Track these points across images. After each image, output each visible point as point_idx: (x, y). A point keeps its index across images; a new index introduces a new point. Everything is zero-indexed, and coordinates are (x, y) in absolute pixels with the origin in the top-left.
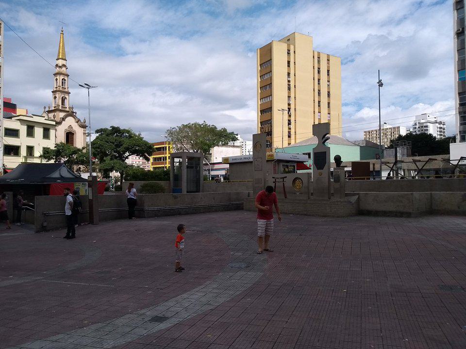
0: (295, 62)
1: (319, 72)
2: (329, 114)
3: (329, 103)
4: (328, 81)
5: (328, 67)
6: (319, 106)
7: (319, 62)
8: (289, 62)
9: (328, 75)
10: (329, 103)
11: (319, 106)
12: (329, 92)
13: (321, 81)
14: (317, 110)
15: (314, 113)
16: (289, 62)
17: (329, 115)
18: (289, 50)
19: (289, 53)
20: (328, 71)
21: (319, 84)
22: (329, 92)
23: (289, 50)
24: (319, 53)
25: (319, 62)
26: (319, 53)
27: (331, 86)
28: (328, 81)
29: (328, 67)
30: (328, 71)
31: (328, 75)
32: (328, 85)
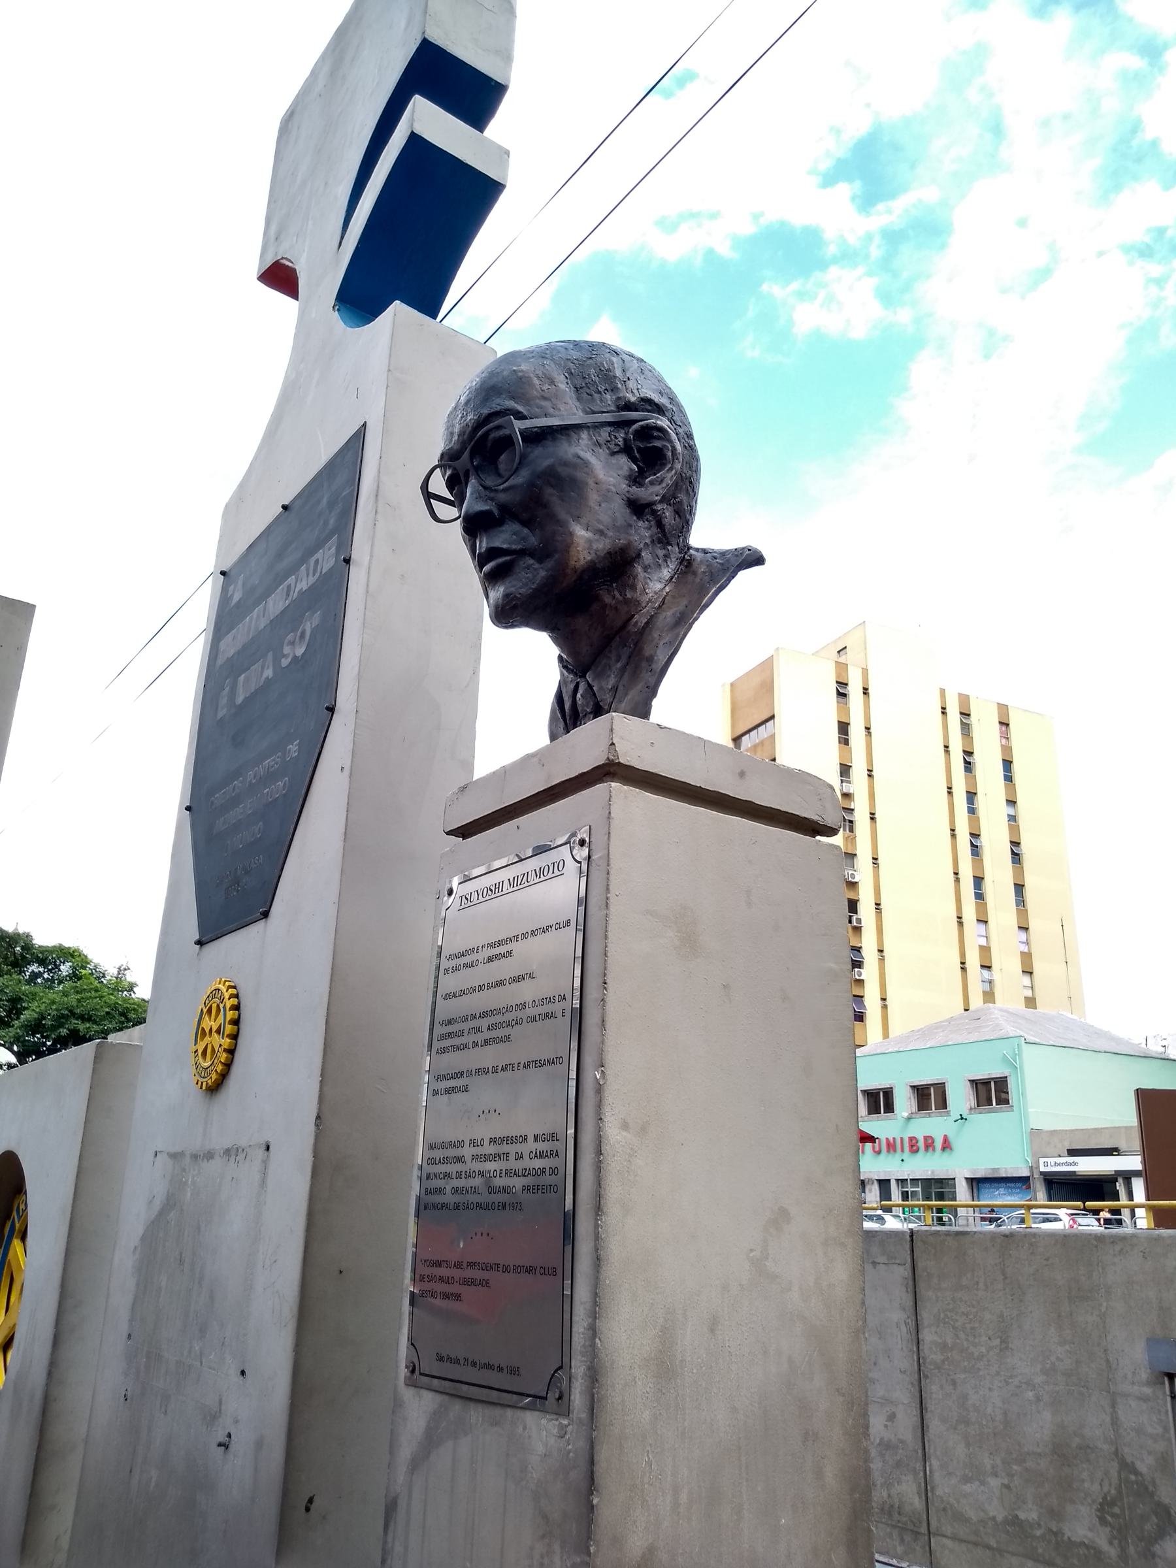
0: (868, 729)
1: (968, 766)
2: (1024, 928)
3: (1019, 888)
4: (1012, 802)
5: (1007, 750)
6: (980, 896)
7: (966, 729)
8: (843, 728)
9: (1009, 778)
10: (1019, 888)
11: (980, 896)
12: (1015, 844)
13: (980, 801)
14: (970, 913)
15: (960, 924)
16: (843, 728)
17: (1023, 936)
18: (842, 684)
19: (842, 695)
20: (1008, 764)
21: (972, 811)
22: (1015, 844)
23: (842, 684)
24: (964, 700)
25: (966, 729)
26: (964, 700)
27: (1022, 822)
28: (1012, 802)
29: (1007, 750)
30: (1008, 764)
31: (1009, 778)
32: (1012, 818)
